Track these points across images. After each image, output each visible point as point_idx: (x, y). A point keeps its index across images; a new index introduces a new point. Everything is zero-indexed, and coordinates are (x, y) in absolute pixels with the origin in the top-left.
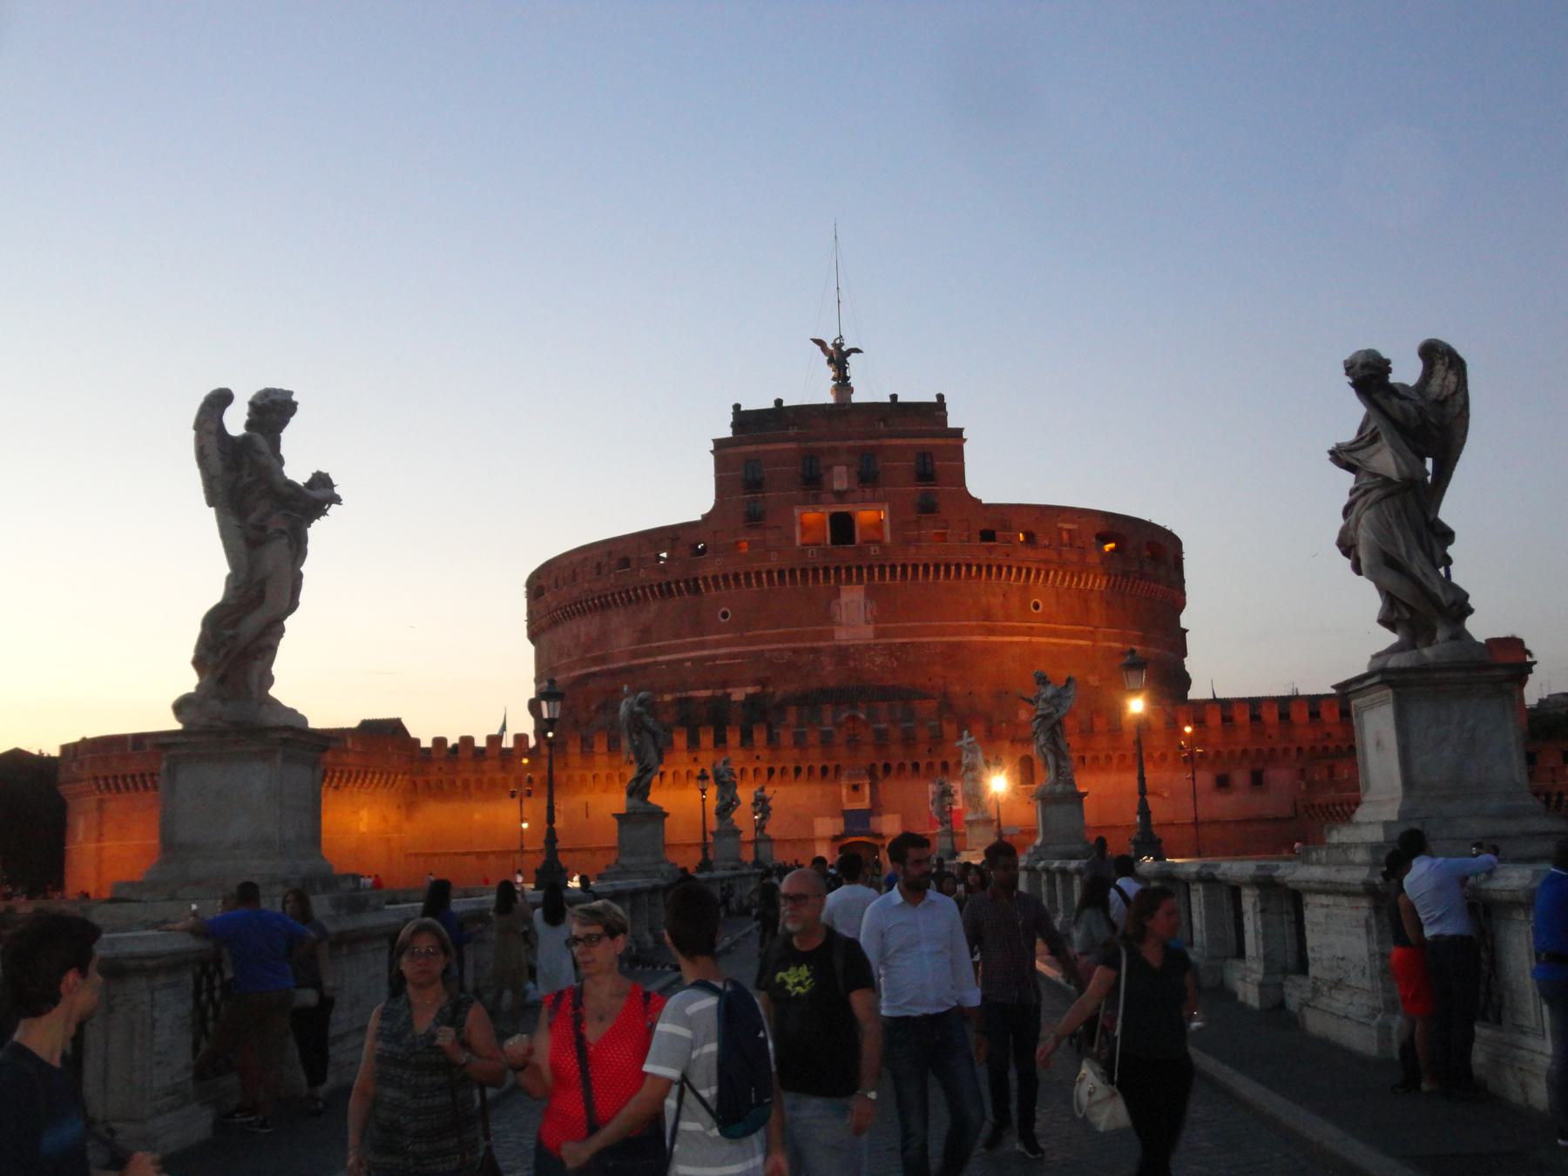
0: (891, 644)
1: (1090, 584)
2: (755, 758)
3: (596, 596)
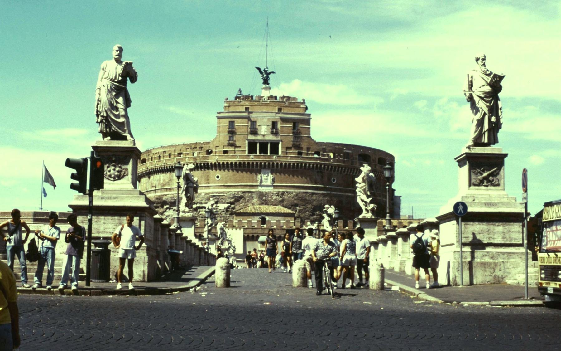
0: (279, 192)
1: (355, 173)
3: (168, 166)
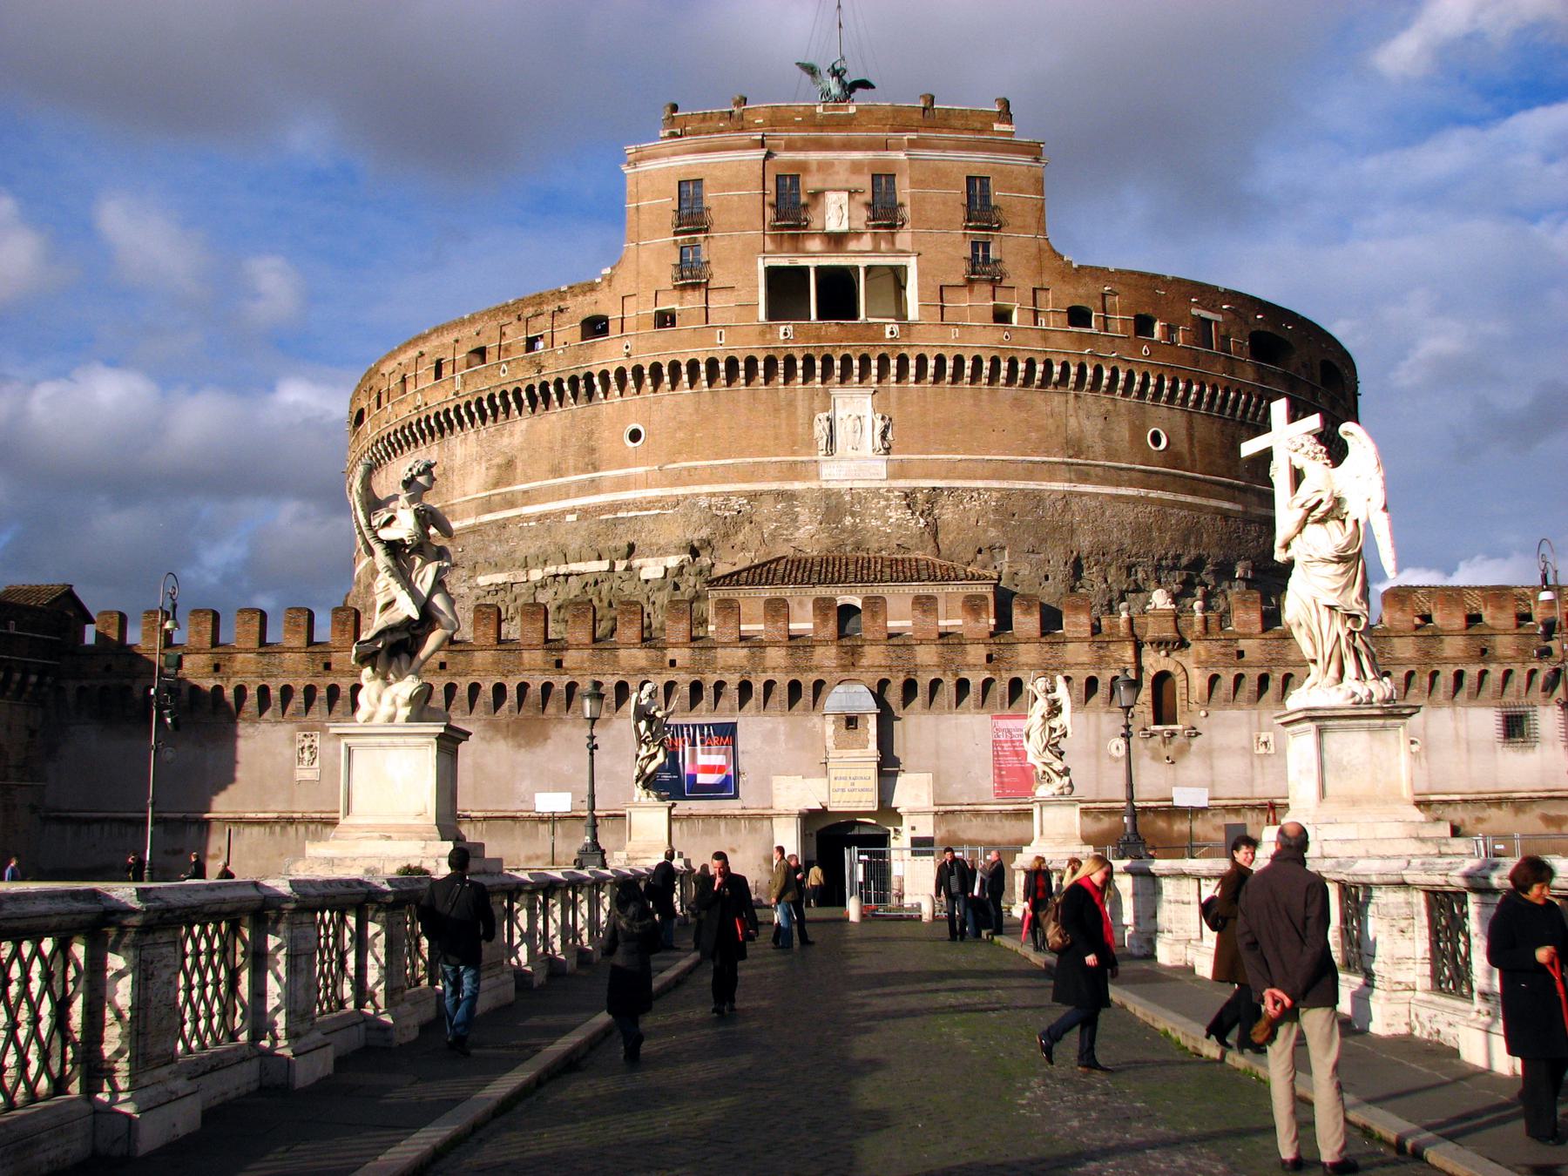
0: (914, 491)
2: (667, 663)
